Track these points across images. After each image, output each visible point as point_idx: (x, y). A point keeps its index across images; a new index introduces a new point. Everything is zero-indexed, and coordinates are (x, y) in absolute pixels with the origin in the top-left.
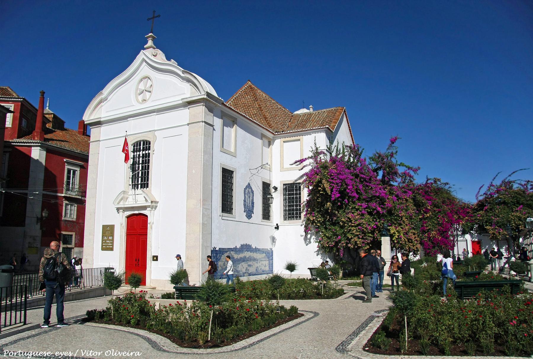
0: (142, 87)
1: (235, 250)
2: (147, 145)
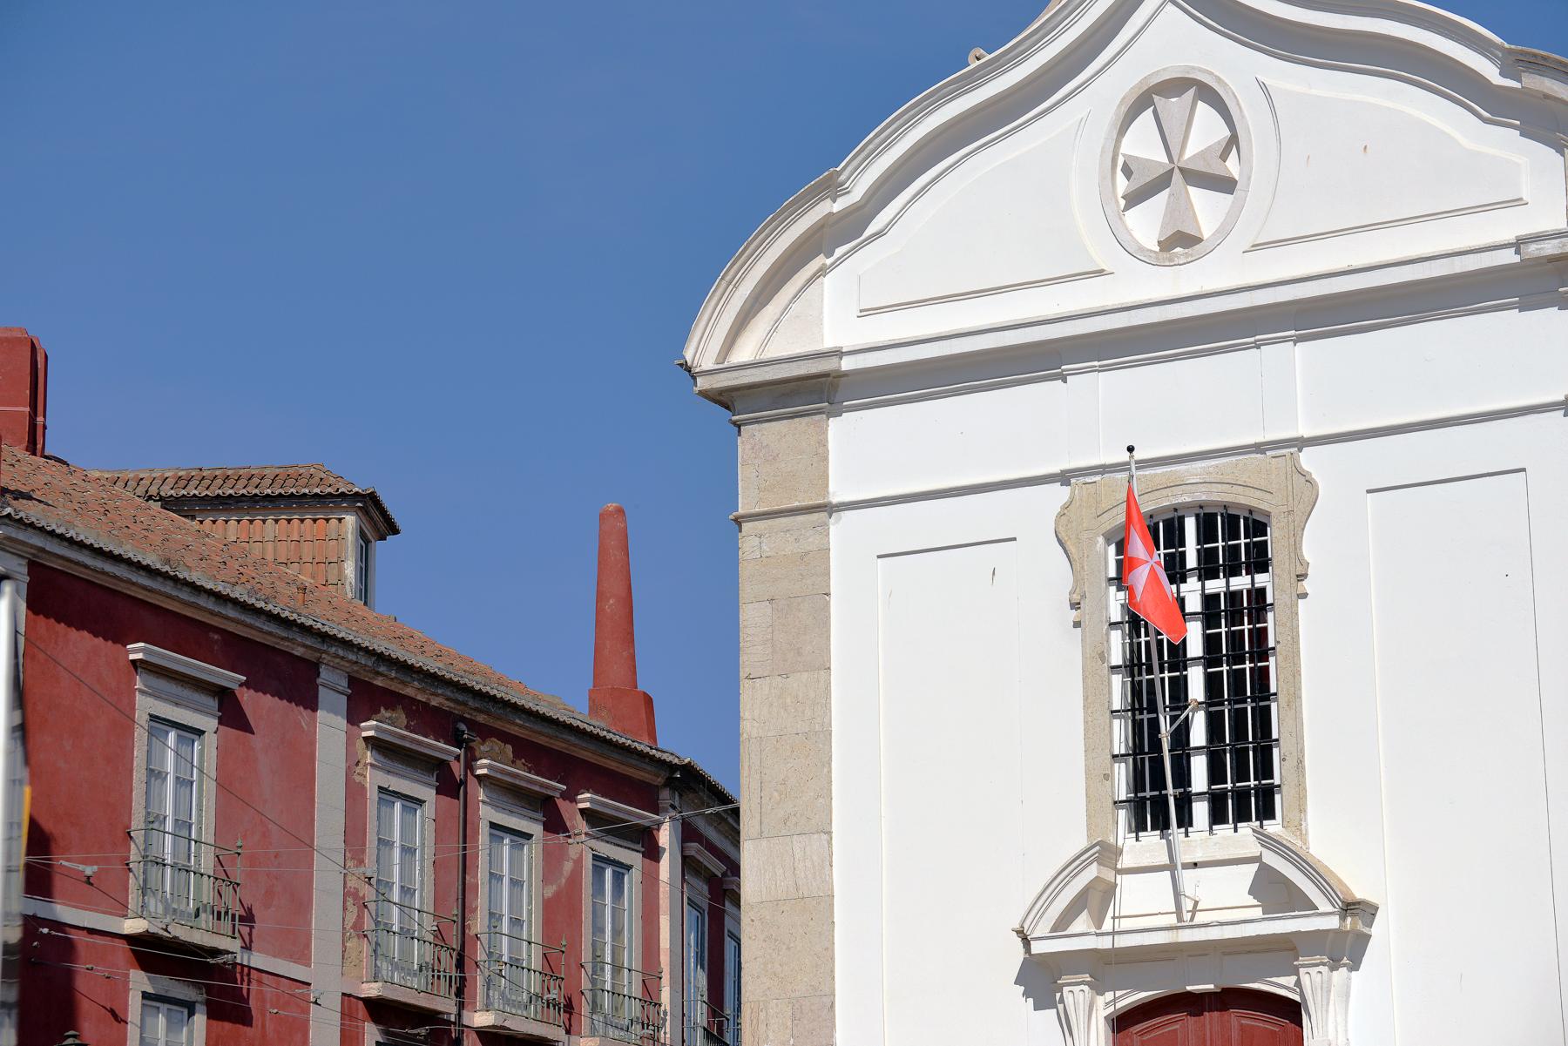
0: (1143, 142)
2: (1237, 538)
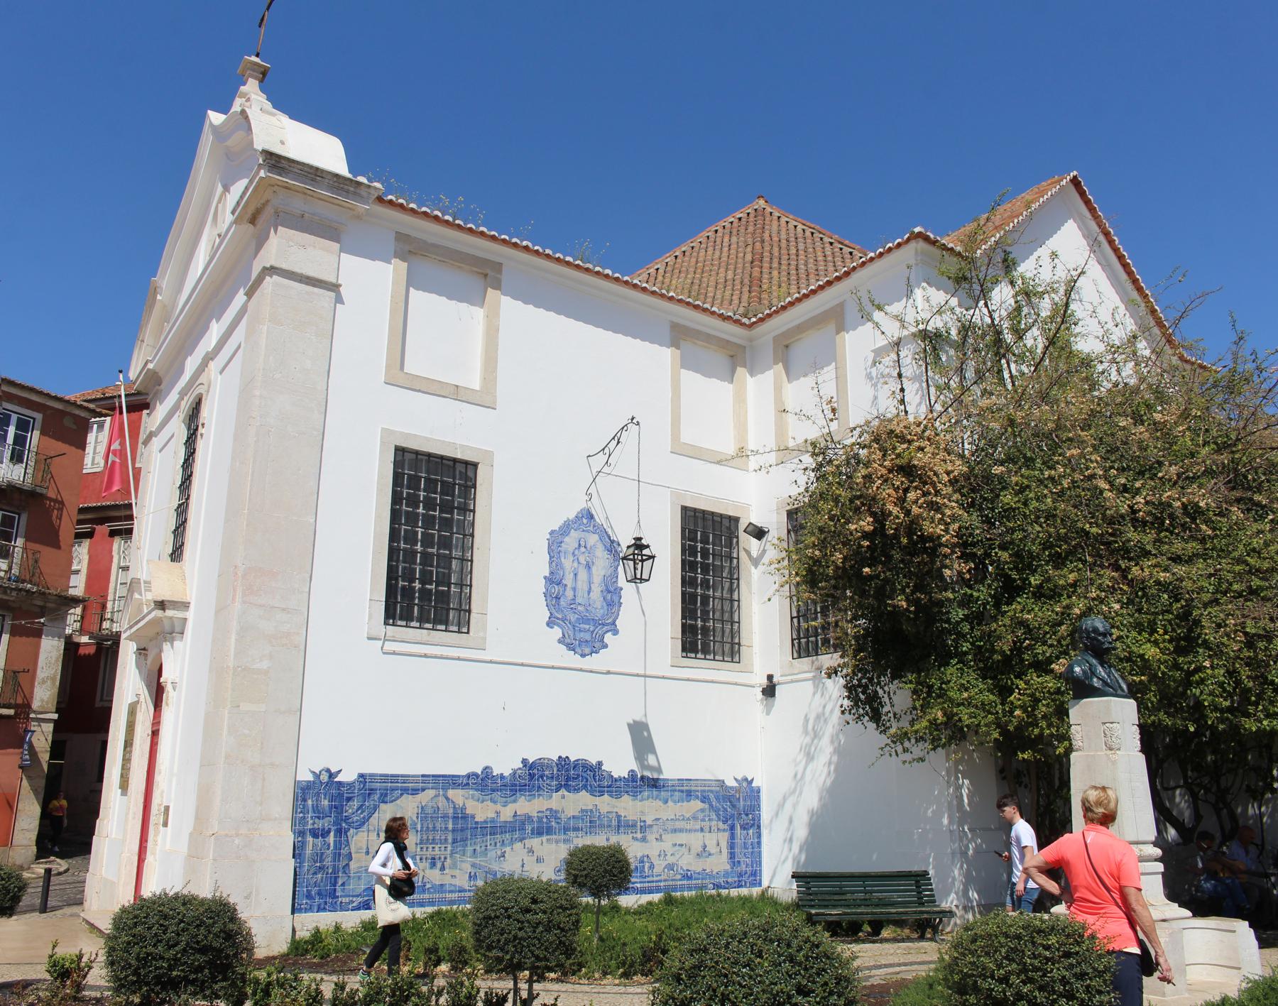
1: (484, 782)
